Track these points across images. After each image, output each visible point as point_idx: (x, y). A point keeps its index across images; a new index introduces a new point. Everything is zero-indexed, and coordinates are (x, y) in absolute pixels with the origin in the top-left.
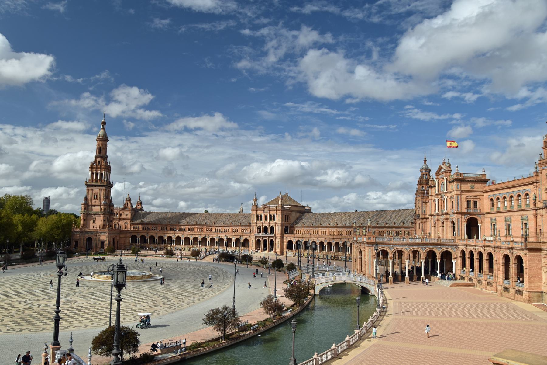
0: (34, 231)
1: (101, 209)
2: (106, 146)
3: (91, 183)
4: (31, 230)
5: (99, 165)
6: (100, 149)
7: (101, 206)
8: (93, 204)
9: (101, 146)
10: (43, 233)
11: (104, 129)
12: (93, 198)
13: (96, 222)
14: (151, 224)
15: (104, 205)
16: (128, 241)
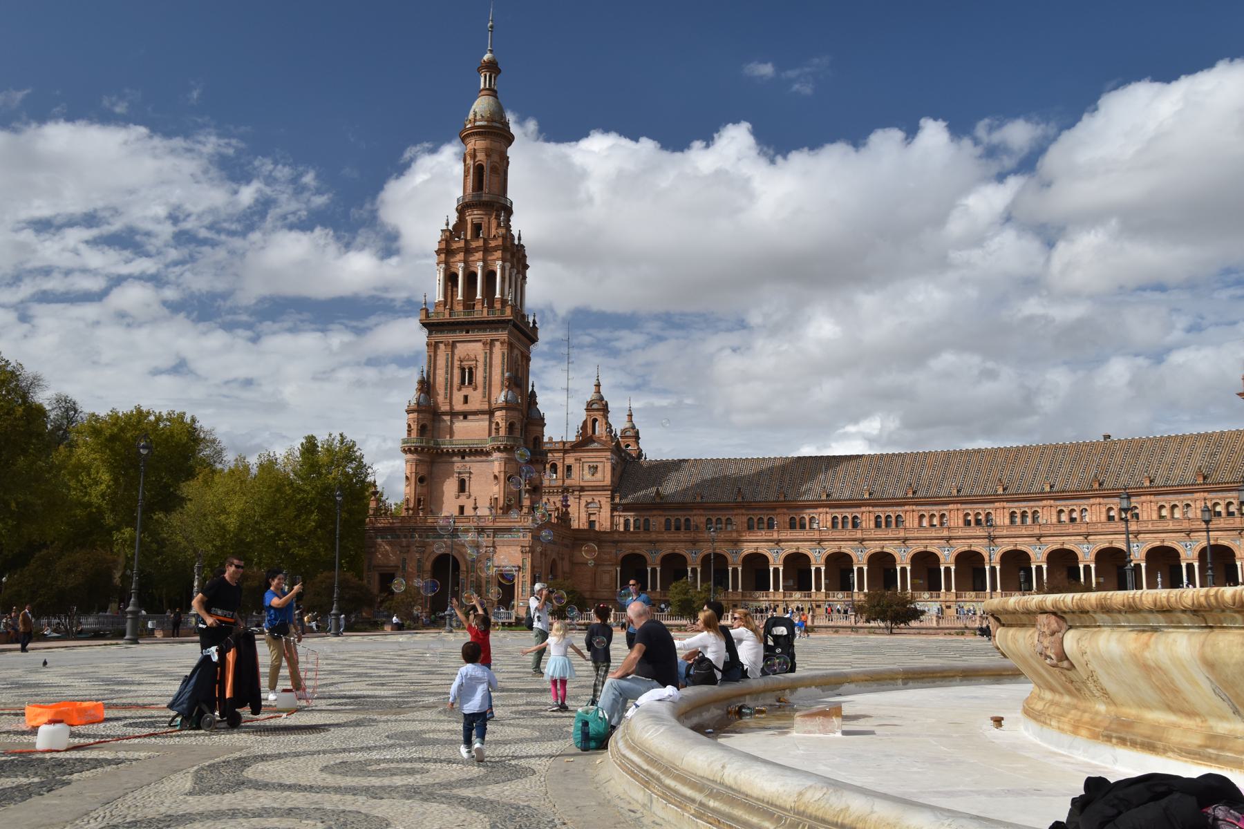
0: (182, 501)
1: (493, 428)
2: (505, 160)
3: (445, 316)
4: (169, 501)
5: (476, 235)
6: (479, 170)
7: (491, 413)
8: (459, 406)
9: (481, 157)
10: (232, 523)
11: (492, 92)
12: (457, 380)
13: (474, 487)
14: (702, 506)
15: (508, 406)
16: (606, 579)
